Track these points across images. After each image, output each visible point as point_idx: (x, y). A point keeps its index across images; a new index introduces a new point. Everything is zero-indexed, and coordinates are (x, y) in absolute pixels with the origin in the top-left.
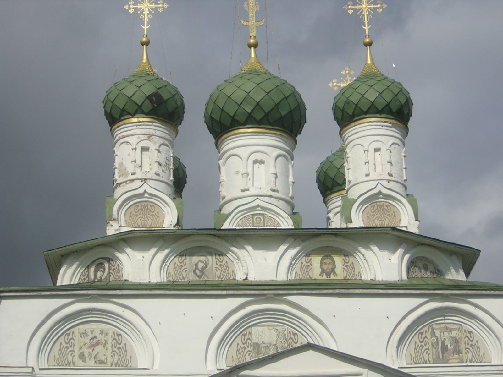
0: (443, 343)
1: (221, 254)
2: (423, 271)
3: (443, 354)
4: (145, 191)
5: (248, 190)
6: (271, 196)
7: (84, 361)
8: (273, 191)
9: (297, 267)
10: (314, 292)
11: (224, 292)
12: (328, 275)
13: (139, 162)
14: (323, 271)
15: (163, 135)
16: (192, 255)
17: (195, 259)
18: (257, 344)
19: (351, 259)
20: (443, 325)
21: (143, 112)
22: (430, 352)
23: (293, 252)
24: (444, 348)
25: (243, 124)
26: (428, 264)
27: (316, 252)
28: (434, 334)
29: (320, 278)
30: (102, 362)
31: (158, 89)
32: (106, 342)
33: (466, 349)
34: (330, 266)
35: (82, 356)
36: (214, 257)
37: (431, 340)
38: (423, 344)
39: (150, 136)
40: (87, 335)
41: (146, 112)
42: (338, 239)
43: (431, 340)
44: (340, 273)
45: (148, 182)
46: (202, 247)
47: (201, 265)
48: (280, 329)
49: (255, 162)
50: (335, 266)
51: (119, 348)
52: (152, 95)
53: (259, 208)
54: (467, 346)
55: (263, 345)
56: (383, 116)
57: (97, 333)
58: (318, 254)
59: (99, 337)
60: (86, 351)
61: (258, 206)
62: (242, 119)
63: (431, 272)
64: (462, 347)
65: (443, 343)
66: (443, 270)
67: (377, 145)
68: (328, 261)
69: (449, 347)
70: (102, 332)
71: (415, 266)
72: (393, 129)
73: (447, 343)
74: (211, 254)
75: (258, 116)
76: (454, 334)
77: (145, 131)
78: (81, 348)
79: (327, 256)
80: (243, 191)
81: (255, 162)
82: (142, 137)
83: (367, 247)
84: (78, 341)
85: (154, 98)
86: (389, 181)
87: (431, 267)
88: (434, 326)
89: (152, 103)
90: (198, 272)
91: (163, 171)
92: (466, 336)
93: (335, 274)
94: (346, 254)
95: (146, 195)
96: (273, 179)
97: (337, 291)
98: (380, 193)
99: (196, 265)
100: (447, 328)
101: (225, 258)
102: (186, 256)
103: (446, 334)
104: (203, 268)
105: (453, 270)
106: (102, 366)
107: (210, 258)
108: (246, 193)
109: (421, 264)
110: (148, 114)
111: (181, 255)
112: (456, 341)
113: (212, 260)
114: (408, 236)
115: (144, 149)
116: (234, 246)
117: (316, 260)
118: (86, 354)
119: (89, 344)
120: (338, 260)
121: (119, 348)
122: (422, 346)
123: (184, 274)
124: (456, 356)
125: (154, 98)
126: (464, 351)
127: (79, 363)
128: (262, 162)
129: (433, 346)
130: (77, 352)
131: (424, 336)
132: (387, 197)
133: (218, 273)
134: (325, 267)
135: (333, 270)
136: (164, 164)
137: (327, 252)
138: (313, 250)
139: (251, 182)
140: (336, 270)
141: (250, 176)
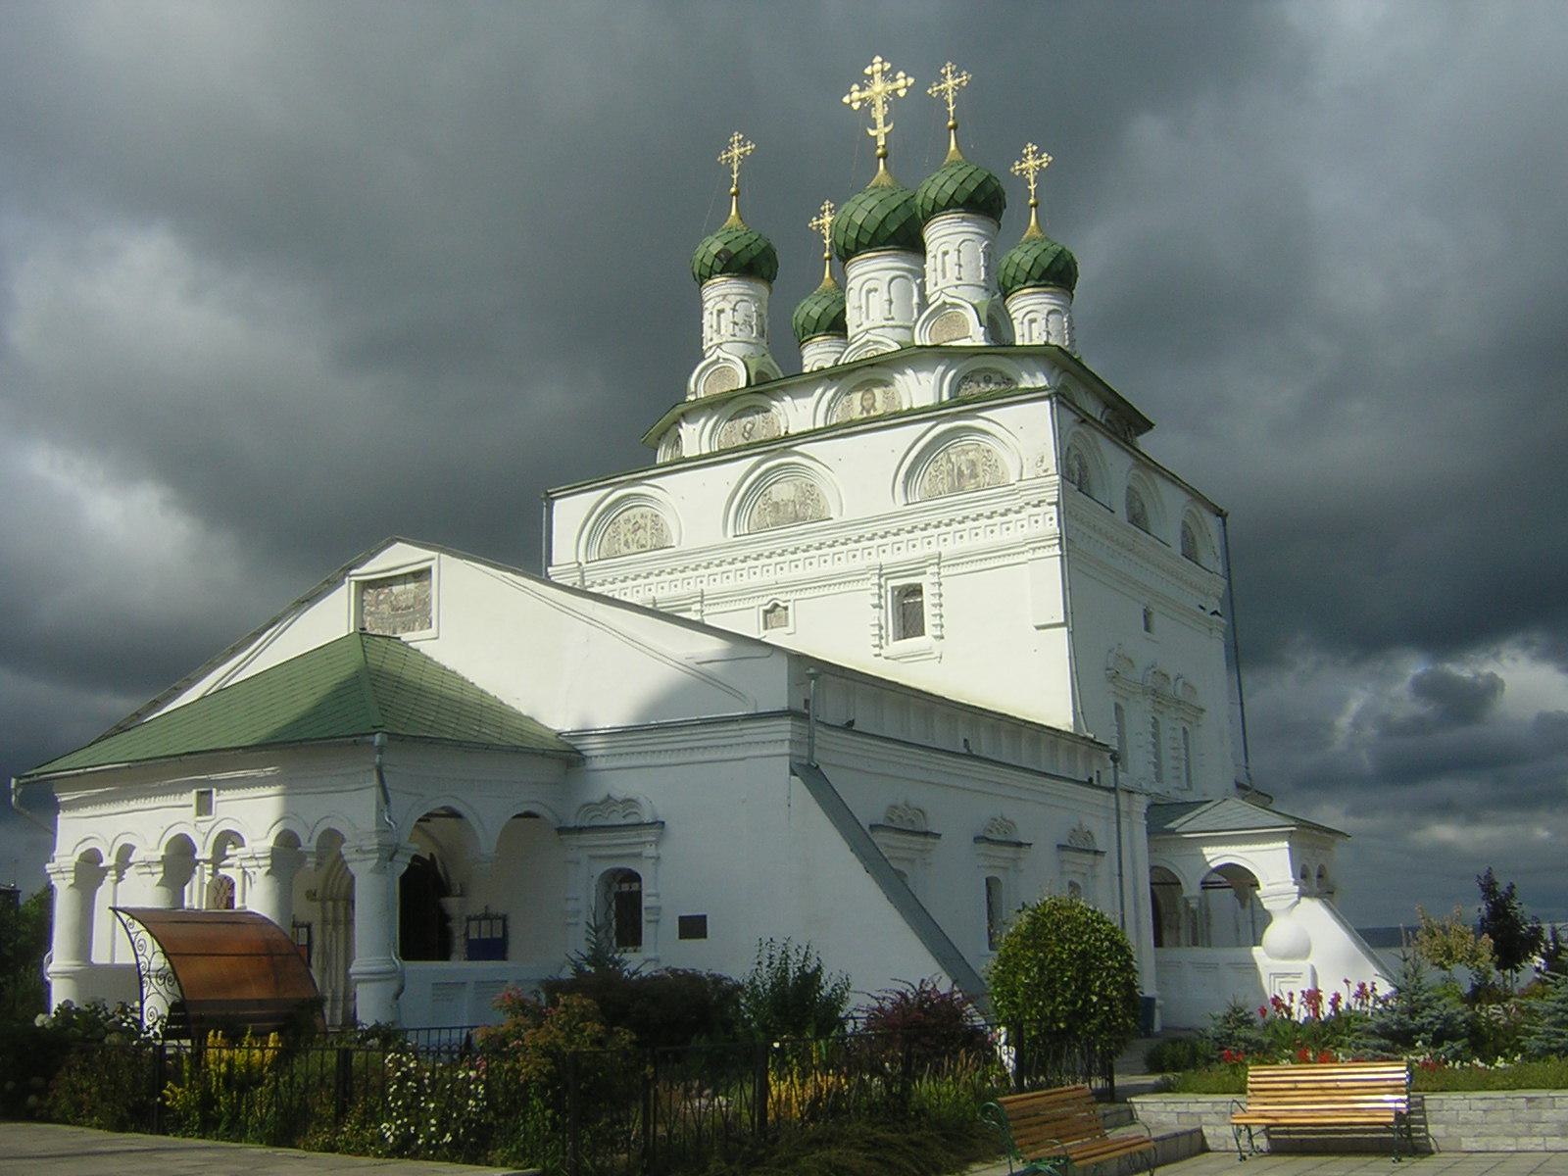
0: (959, 468)
1: (768, 411)
2: (982, 385)
3: (959, 480)
4: (719, 358)
5: (861, 324)
6: (884, 327)
7: (629, 548)
8: (888, 319)
9: (839, 409)
10: (828, 435)
11: (747, 453)
12: (868, 412)
13: (715, 327)
14: (863, 408)
15: (741, 291)
16: (740, 417)
17: (744, 420)
18: (777, 503)
19: (891, 388)
20: (960, 449)
21: (716, 273)
22: (945, 481)
23: (830, 394)
24: (961, 474)
25: (855, 252)
26: (992, 376)
27: (856, 389)
28: (949, 460)
29: (861, 417)
30: (643, 546)
31: (726, 244)
32: (646, 525)
33: (984, 470)
34: (871, 402)
35: (626, 544)
36: (761, 415)
37: (946, 467)
38: (938, 473)
39: (725, 296)
40: (630, 521)
41: (718, 270)
42: (874, 369)
43: (946, 467)
44: (880, 408)
45: (723, 347)
46: (749, 407)
47: (749, 426)
48: (797, 483)
49: (869, 292)
50: (875, 401)
51: (656, 530)
52: (719, 252)
53: (871, 343)
54: (986, 468)
55: (782, 503)
56: (951, 211)
57: (638, 519)
58: (859, 390)
59: (641, 522)
60: (630, 537)
61: (868, 341)
62: (851, 246)
63: (996, 384)
64: (979, 470)
65: (959, 468)
66: (1014, 376)
67: (943, 248)
68: (867, 396)
69: (965, 472)
70: (642, 516)
71: (971, 381)
72: (965, 224)
73: (963, 468)
74: (758, 413)
75: (865, 240)
76: (971, 455)
77: (718, 293)
78: (625, 535)
79: (867, 390)
80: (858, 327)
81: (869, 292)
82: (717, 299)
83: (903, 373)
84: (624, 528)
85: (723, 256)
86: (956, 287)
87: (998, 378)
88: (950, 451)
89: (721, 260)
90: (746, 434)
91: (741, 330)
92: (984, 457)
93: (875, 410)
94: (886, 383)
95: (721, 360)
96: (887, 307)
97: (840, 432)
98: (945, 303)
99: (745, 427)
100: (963, 450)
101: (770, 414)
102: (736, 419)
103: (963, 457)
104: (751, 429)
105: (1026, 376)
106: (644, 549)
107: (756, 416)
108: (861, 329)
109: (980, 378)
110: (722, 273)
111: (731, 420)
112: (973, 464)
113: (759, 418)
114: (951, 350)
115: (720, 312)
116: (775, 400)
117: (857, 396)
118: (630, 540)
119: (632, 531)
120: (878, 392)
121: (656, 530)
122: (937, 476)
123: (734, 439)
124: (973, 481)
125: (723, 256)
126: (981, 474)
127: (625, 550)
128: (876, 290)
129: (948, 473)
130: (622, 542)
131: (939, 463)
132: (954, 306)
133: (764, 432)
134: (865, 404)
135: (873, 404)
136: (741, 322)
137: (867, 385)
138: (854, 387)
139: (864, 316)
140: (876, 404)
141: (864, 309)
